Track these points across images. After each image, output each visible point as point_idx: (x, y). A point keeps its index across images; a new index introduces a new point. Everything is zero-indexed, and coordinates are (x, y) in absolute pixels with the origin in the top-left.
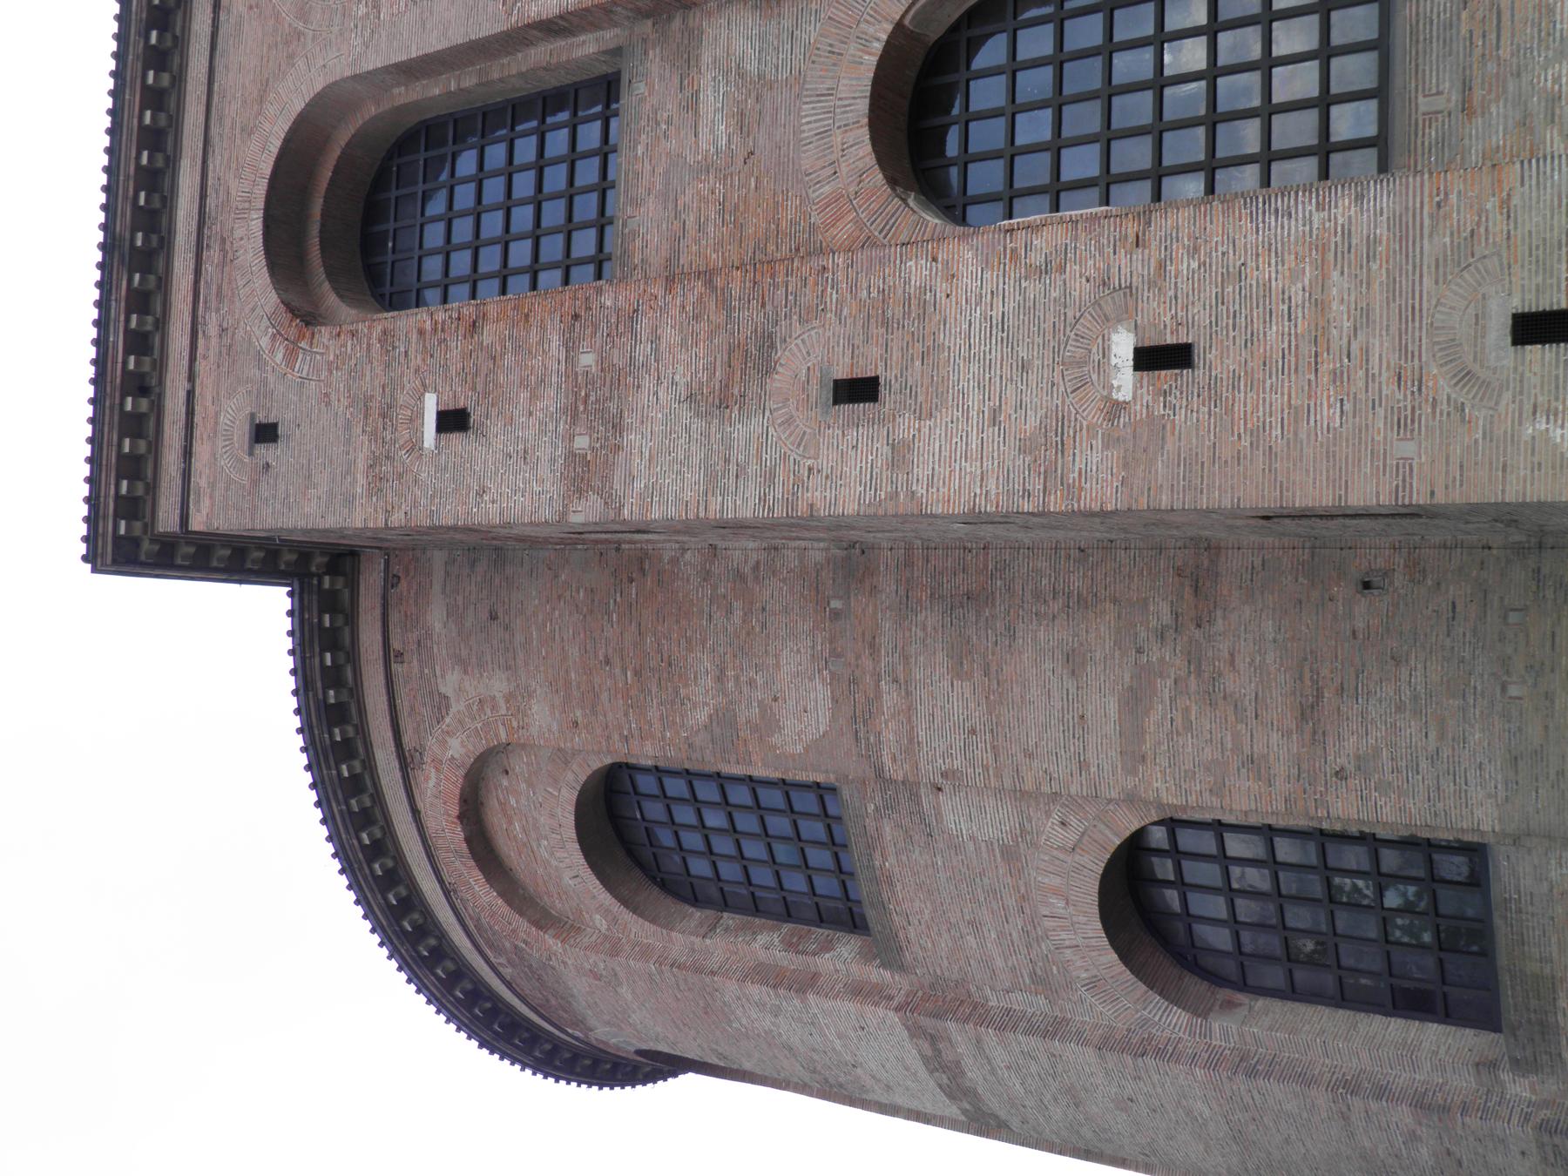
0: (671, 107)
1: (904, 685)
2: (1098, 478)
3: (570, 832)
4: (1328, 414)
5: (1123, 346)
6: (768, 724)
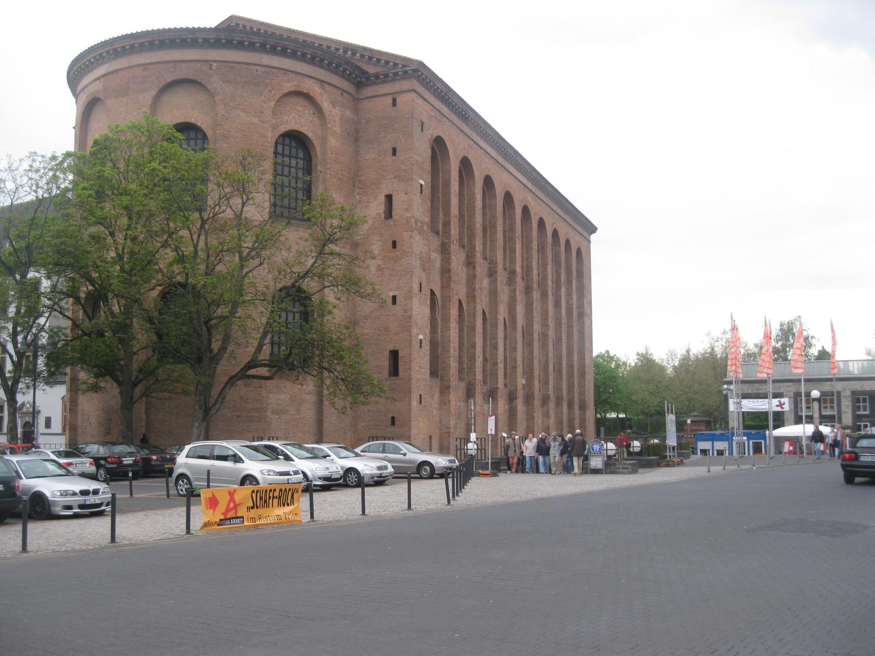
2: (414, 331)
3: (300, 130)
5: (421, 337)
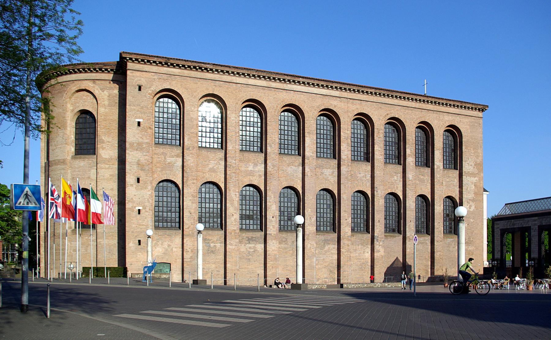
0: (173, 154)
1: (108, 168)
4: (134, 226)
5: (141, 208)
6: (103, 149)
